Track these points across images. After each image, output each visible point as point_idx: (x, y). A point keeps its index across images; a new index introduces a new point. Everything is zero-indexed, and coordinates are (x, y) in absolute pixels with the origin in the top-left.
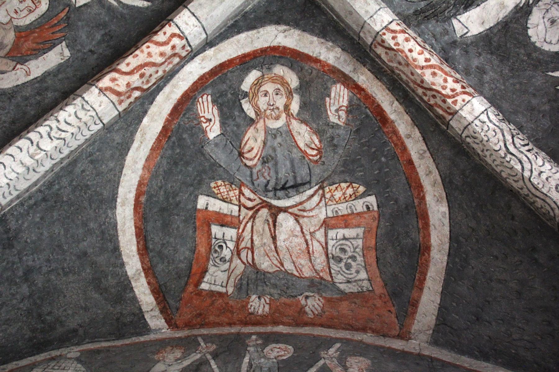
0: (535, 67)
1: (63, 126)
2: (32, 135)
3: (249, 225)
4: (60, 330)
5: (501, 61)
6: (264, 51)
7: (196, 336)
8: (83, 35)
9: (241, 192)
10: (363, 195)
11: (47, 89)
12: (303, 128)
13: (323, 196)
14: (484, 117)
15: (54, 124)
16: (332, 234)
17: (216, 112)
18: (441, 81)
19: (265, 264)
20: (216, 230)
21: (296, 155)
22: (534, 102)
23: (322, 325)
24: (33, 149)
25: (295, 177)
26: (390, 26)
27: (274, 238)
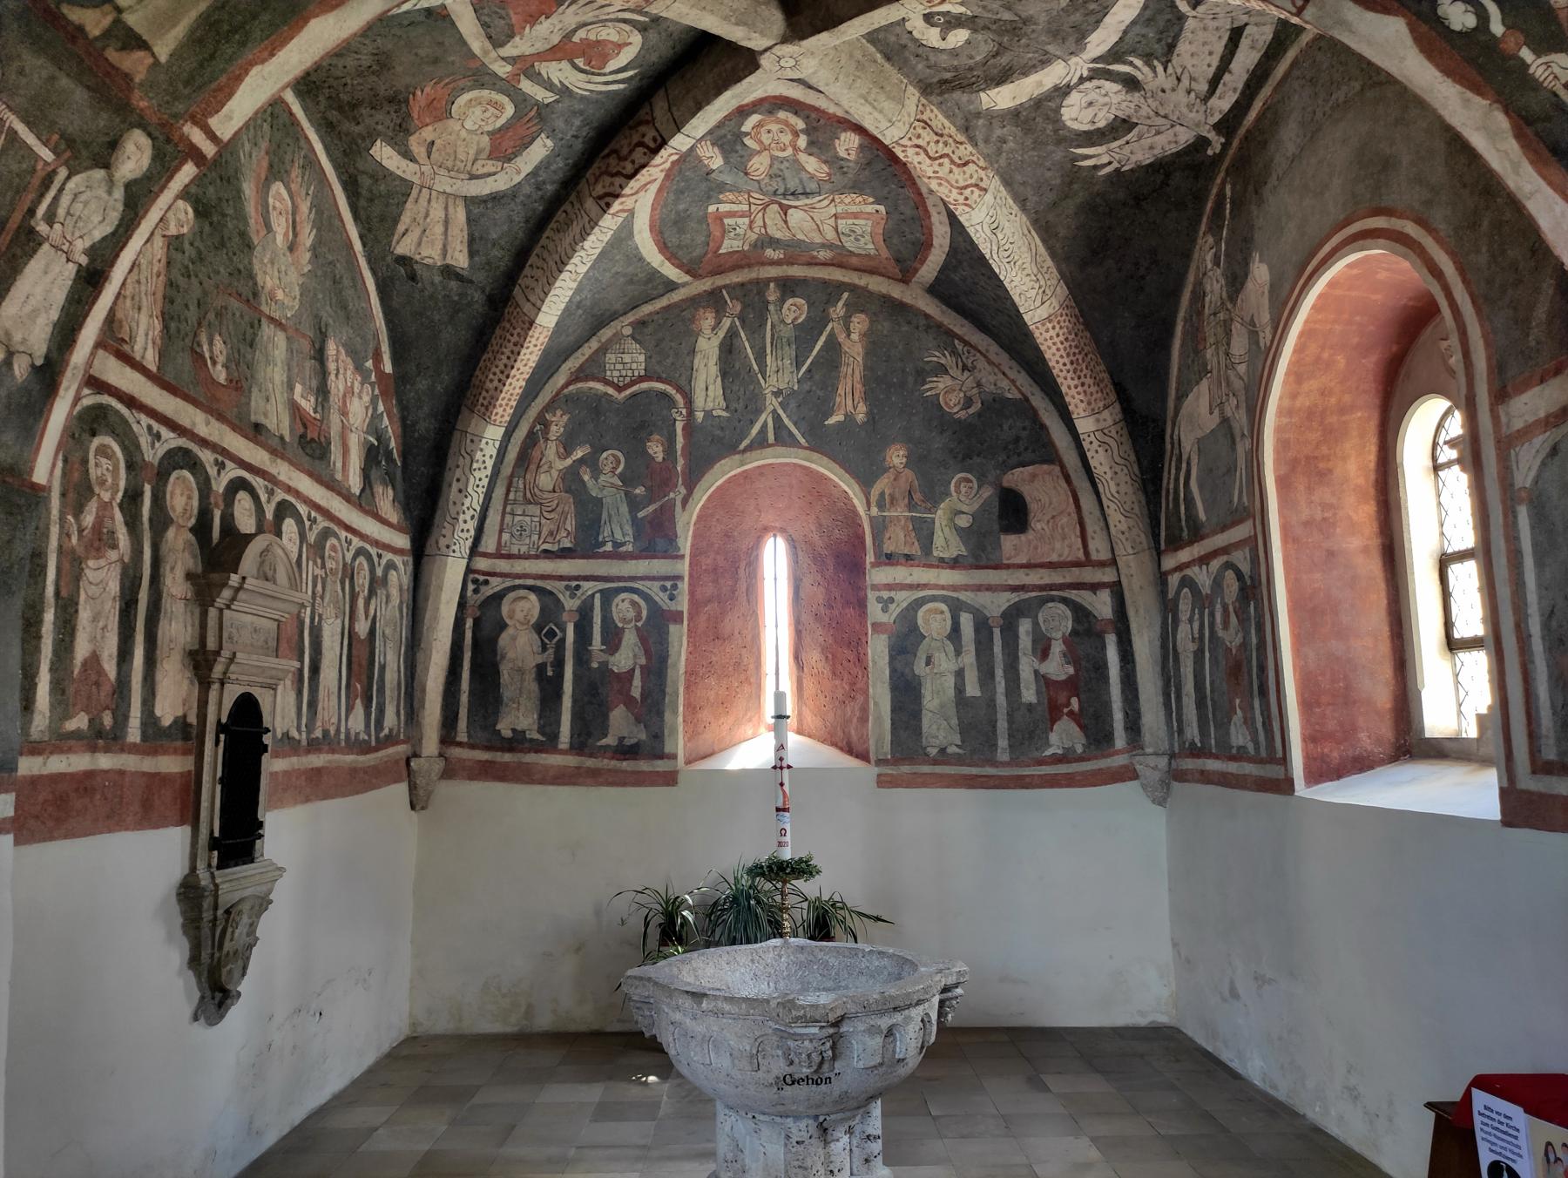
0: (1060, 141)
1: (591, 251)
2: (568, 268)
3: (760, 214)
4: (608, 313)
5: (1026, 134)
6: (761, 101)
7: (720, 289)
8: (560, 124)
9: (750, 196)
10: (873, 203)
11: (544, 183)
12: (812, 159)
13: (833, 200)
14: (979, 227)
15: (582, 253)
16: (840, 221)
17: (716, 149)
18: (946, 192)
19: (778, 235)
20: (726, 221)
21: (804, 176)
22: (1049, 174)
23: (833, 265)
24: (573, 276)
25: (804, 188)
26: (901, 142)
27: (786, 222)
